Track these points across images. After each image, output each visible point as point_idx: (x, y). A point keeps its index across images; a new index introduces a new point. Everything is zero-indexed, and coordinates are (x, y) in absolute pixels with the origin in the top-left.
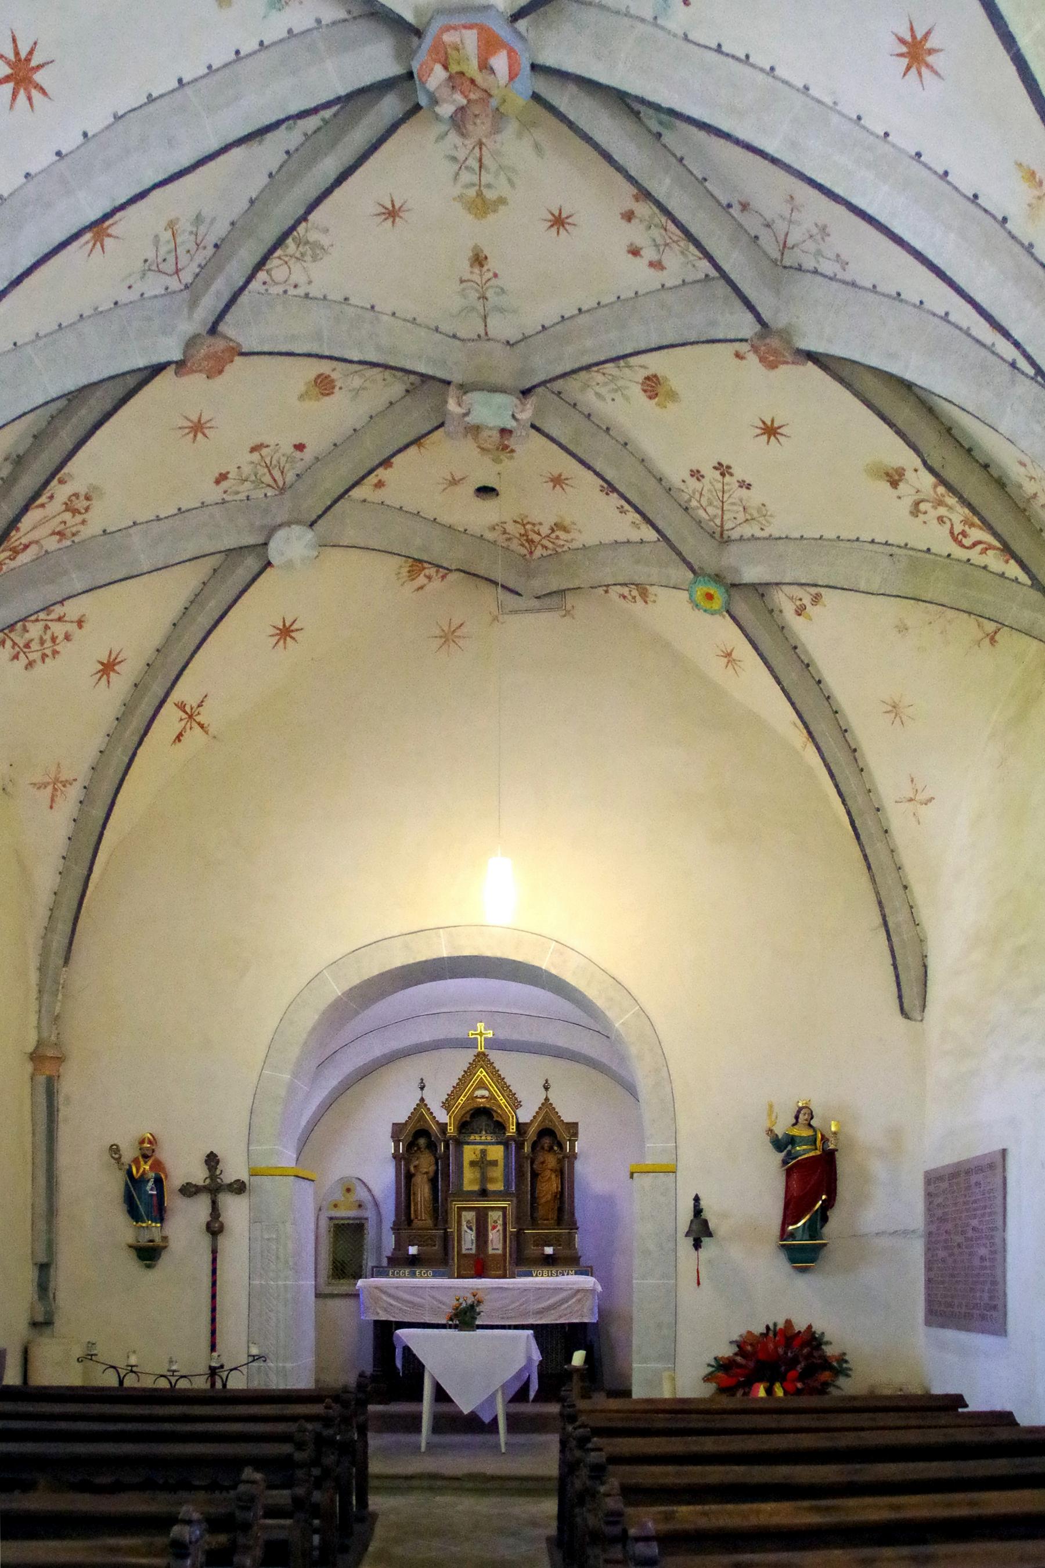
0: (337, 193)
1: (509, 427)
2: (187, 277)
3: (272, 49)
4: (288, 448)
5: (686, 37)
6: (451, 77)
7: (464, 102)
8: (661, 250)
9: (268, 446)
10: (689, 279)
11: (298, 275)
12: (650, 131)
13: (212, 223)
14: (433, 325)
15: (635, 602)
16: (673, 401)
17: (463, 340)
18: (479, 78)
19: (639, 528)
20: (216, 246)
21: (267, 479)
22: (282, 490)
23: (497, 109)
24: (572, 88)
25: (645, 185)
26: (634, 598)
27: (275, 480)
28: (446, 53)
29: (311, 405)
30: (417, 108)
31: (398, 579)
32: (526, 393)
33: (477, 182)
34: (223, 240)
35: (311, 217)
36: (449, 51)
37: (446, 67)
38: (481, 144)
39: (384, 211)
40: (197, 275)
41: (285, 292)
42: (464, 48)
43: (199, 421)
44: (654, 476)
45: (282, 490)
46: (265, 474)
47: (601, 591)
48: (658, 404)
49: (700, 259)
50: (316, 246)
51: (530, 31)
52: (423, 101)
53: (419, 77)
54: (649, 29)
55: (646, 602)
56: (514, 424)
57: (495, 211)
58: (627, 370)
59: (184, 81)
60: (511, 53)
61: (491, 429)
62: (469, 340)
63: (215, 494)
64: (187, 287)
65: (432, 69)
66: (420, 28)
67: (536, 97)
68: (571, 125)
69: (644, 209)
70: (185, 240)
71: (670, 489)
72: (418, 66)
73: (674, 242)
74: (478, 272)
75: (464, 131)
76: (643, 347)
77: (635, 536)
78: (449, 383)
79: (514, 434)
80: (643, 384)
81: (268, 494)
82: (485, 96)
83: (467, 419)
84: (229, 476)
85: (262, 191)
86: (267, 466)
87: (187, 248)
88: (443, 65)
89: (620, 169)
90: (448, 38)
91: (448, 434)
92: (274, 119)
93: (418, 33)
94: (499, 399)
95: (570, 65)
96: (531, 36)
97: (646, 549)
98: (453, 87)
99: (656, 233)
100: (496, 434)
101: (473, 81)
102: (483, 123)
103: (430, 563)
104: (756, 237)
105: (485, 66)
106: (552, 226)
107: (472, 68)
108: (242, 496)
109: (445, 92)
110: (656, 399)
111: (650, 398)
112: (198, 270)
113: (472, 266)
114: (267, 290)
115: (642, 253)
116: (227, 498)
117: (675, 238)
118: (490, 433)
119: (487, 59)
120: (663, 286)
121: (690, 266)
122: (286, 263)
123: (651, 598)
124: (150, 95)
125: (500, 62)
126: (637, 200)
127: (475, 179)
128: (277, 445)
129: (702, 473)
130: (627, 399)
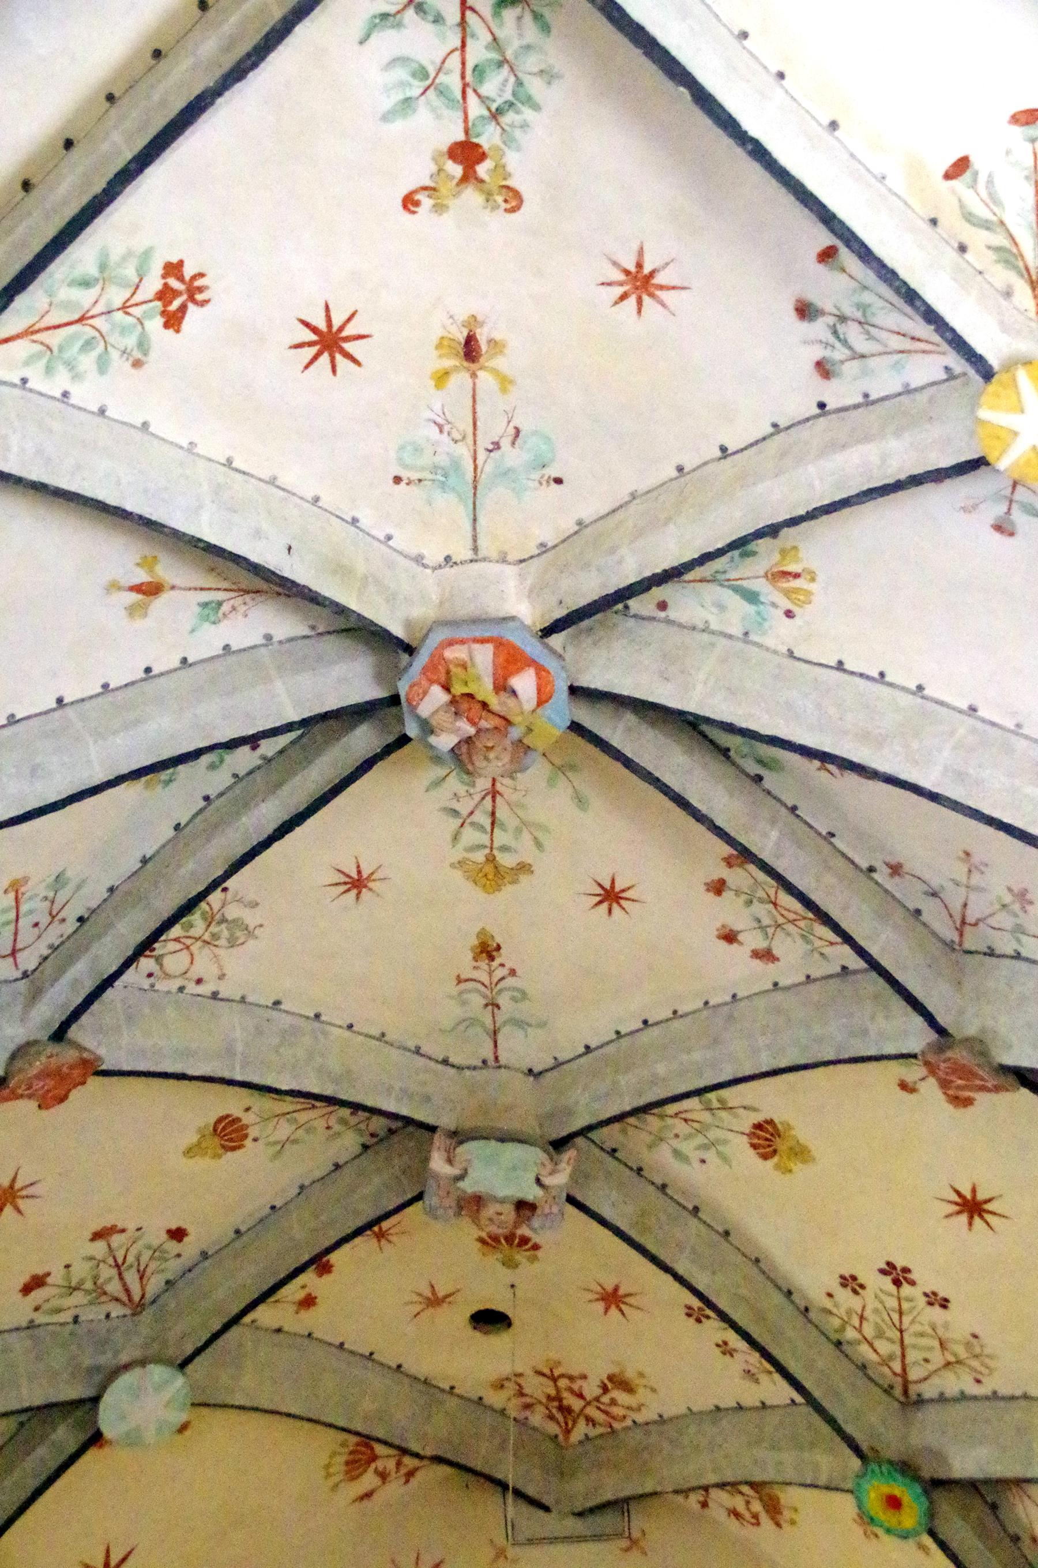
0: (276, 846)
1: (530, 1198)
2: (28, 960)
3: (198, 669)
4: (157, 1236)
5: (791, 654)
6: (453, 702)
7: (472, 731)
8: (770, 935)
9: (123, 1231)
10: (815, 974)
11: (204, 964)
12: (747, 775)
13: (79, 887)
14: (411, 1044)
15: (758, 1524)
16: (805, 1161)
17: (459, 1068)
18: (494, 702)
19: (757, 1381)
20: (81, 920)
21: (114, 1288)
22: (138, 1308)
23: (520, 741)
24: (630, 718)
25: (742, 839)
26: (755, 1516)
27: (127, 1291)
28: (448, 672)
29: (201, 1164)
30: (403, 740)
31: (328, 1475)
32: (559, 1145)
33: (488, 844)
34: (94, 911)
35: (230, 883)
36: (454, 670)
37: (447, 688)
38: (494, 793)
39: (344, 879)
40: (46, 958)
41: (181, 989)
42: (473, 665)
43: (12, 1187)
44: (780, 1289)
45: (138, 1308)
46: (110, 1279)
47: (694, 1498)
48: (777, 1167)
49: (832, 944)
50: (237, 923)
51: (568, 648)
52: (412, 730)
53: (408, 700)
54: (740, 645)
55: (778, 1525)
56: (539, 1192)
57: (515, 882)
58: (723, 1114)
59: (66, 701)
60: (541, 670)
61: (502, 1201)
62: (468, 1068)
63: (20, 1311)
64: (25, 975)
65: (425, 693)
66: (414, 644)
67: (576, 727)
68: (628, 763)
69: (740, 877)
70: (34, 907)
71: (807, 1309)
72: (407, 688)
73: (789, 921)
74: (486, 967)
75: (470, 767)
76: (748, 1072)
77: (751, 1395)
78: (432, 1129)
79: (539, 1212)
80: (751, 1135)
81: (113, 1315)
82: (504, 722)
83: (461, 1184)
84: (49, 1280)
85: (164, 846)
86: (117, 1266)
87: (35, 920)
88: (443, 687)
89: (699, 817)
90: (449, 654)
91: (431, 1213)
92: (191, 748)
93: (410, 650)
94: (513, 1152)
95: (625, 688)
96: (570, 654)
97: (772, 1419)
98: (456, 713)
99: (762, 910)
100: (509, 1213)
101: (484, 705)
102: (497, 758)
103: (385, 1443)
104: (918, 912)
105: (502, 687)
106: (600, 902)
107: (485, 689)
108: (66, 1317)
109: (445, 718)
110: (776, 1159)
111: (765, 1157)
112: (46, 952)
113: (475, 959)
114: (152, 986)
115: (740, 937)
116: (40, 1318)
117: (792, 916)
118: (498, 1207)
119: (505, 679)
120: (776, 984)
121: (816, 955)
122: (188, 948)
123: (787, 1514)
124: (13, 716)
125: (525, 683)
126: (730, 865)
127: (485, 839)
128: (139, 1229)
129: (861, 1280)
130: (725, 1159)
